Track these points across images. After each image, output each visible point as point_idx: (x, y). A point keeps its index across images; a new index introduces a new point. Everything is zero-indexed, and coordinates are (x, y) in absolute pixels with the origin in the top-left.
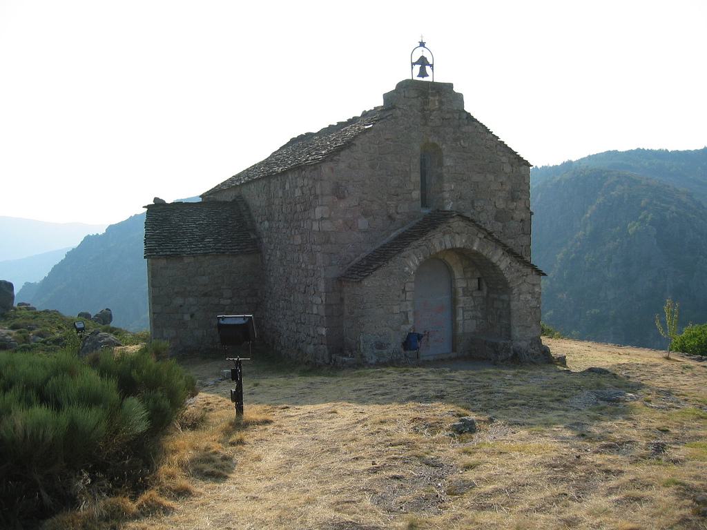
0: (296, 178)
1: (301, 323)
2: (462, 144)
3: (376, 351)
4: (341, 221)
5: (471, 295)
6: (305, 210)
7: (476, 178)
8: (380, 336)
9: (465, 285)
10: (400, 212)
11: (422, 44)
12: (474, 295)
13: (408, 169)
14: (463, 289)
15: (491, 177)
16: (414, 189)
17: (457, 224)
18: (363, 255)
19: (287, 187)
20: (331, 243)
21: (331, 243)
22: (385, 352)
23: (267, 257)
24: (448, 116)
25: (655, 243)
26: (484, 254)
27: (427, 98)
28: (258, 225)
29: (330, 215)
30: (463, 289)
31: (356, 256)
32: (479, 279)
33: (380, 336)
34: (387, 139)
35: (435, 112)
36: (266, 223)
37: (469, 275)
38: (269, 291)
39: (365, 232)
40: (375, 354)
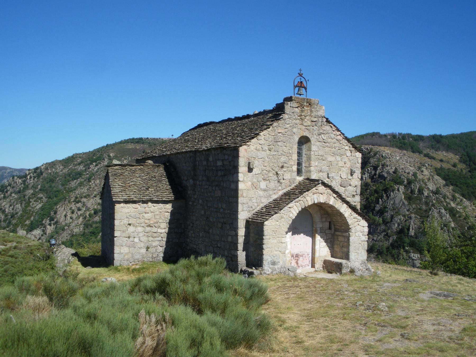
0: (218, 154)
1: (218, 247)
2: (323, 137)
3: (271, 266)
4: (250, 183)
5: (325, 232)
6: (225, 175)
7: (330, 158)
8: (274, 257)
9: (321, 226)
10: (285, 178)
11: (300, 75)
12: (327, 232)
13: (291, 152)
14: (320, 228)
15: (338, 158)
16: (294, 165)
17: (321, 188)
18: (262, 205)
19: (211, 159)
20: (244, 197)
21: (244, 197)
22: (276, 267)
23: (191, 203)
24: (315, 119)
25: (403, 197)
26: (336, 207)
27: (303, 108)
28: (184, 182)
29: (244, 179)
30: (320, 228)
31: (258, 206)
32: (330, 222)
33: (274, 257)
34: (279, 133)
35: (308, 117)
36: (191, 181)
37: (324, 220)
38: (191, 225)
39: (265, 190)
40: (270, 268)
